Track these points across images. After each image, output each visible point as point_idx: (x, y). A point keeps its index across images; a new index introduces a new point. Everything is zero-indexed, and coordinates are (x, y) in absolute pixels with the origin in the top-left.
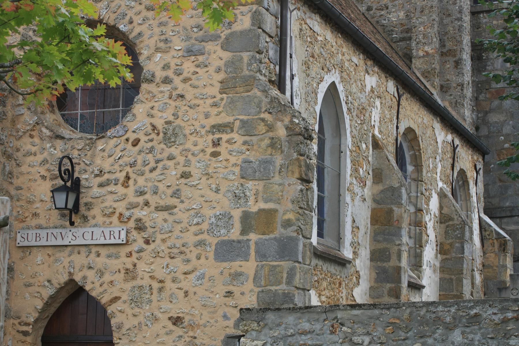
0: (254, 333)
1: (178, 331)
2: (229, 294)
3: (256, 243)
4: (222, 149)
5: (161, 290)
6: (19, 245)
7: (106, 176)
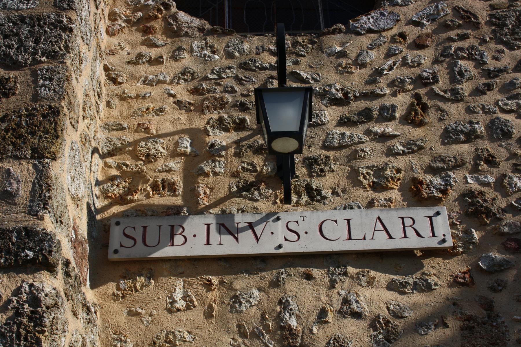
6: (116, 257)
7: (361, 105)
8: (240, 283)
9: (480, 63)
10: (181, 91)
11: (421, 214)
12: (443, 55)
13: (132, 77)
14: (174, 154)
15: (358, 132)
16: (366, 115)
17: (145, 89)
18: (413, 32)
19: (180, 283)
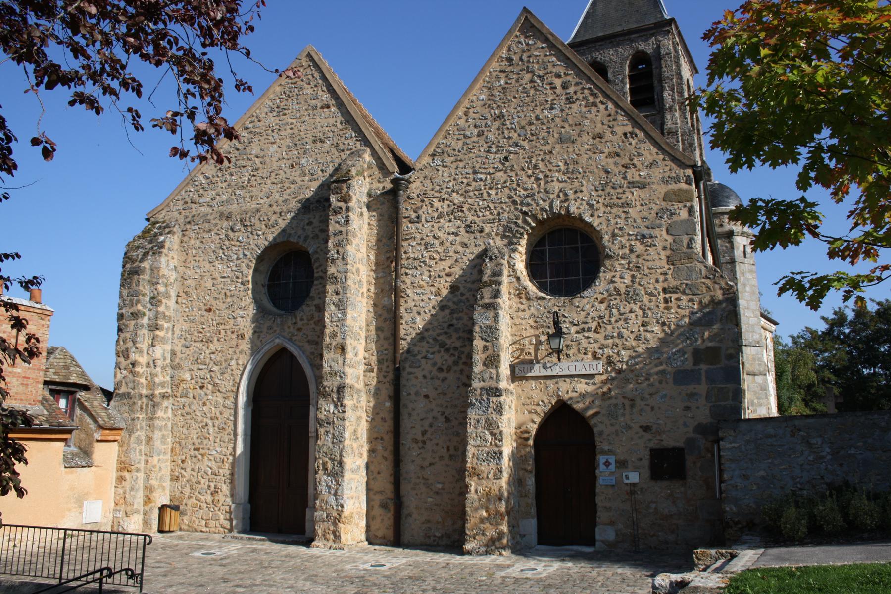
0: (731, 438)
1: (648, 436)
2: (687, 408)
3: (706, 372)
4: (673, 304)
5: (632, 406)
7: (582, 326)
8: (548, 382)
9: (619, 310)
10: (531, 322)
11: (595, 363)
12: (609, 307)
13: (518, 317)
14: (531, 344)
15: (580, 336)
16: (583, 330)
17: (521, 321)
18: (600, 297)
19: (533, 382)
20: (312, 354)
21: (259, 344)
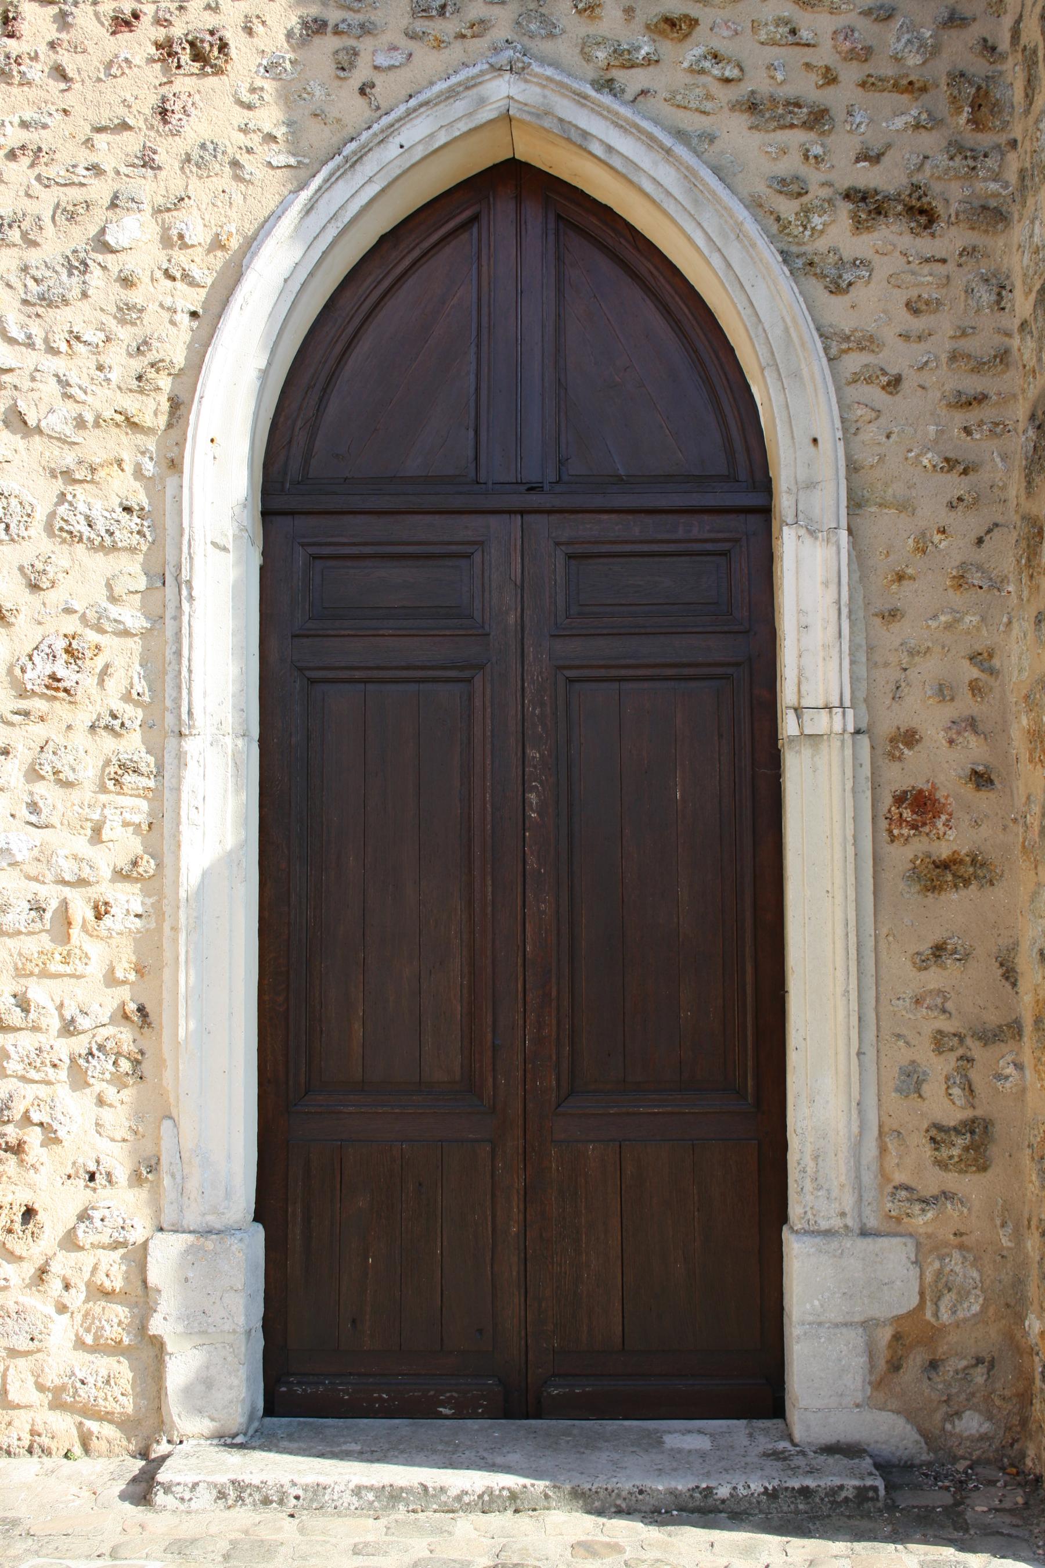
20: (791, 187)
21: (350, 107)
